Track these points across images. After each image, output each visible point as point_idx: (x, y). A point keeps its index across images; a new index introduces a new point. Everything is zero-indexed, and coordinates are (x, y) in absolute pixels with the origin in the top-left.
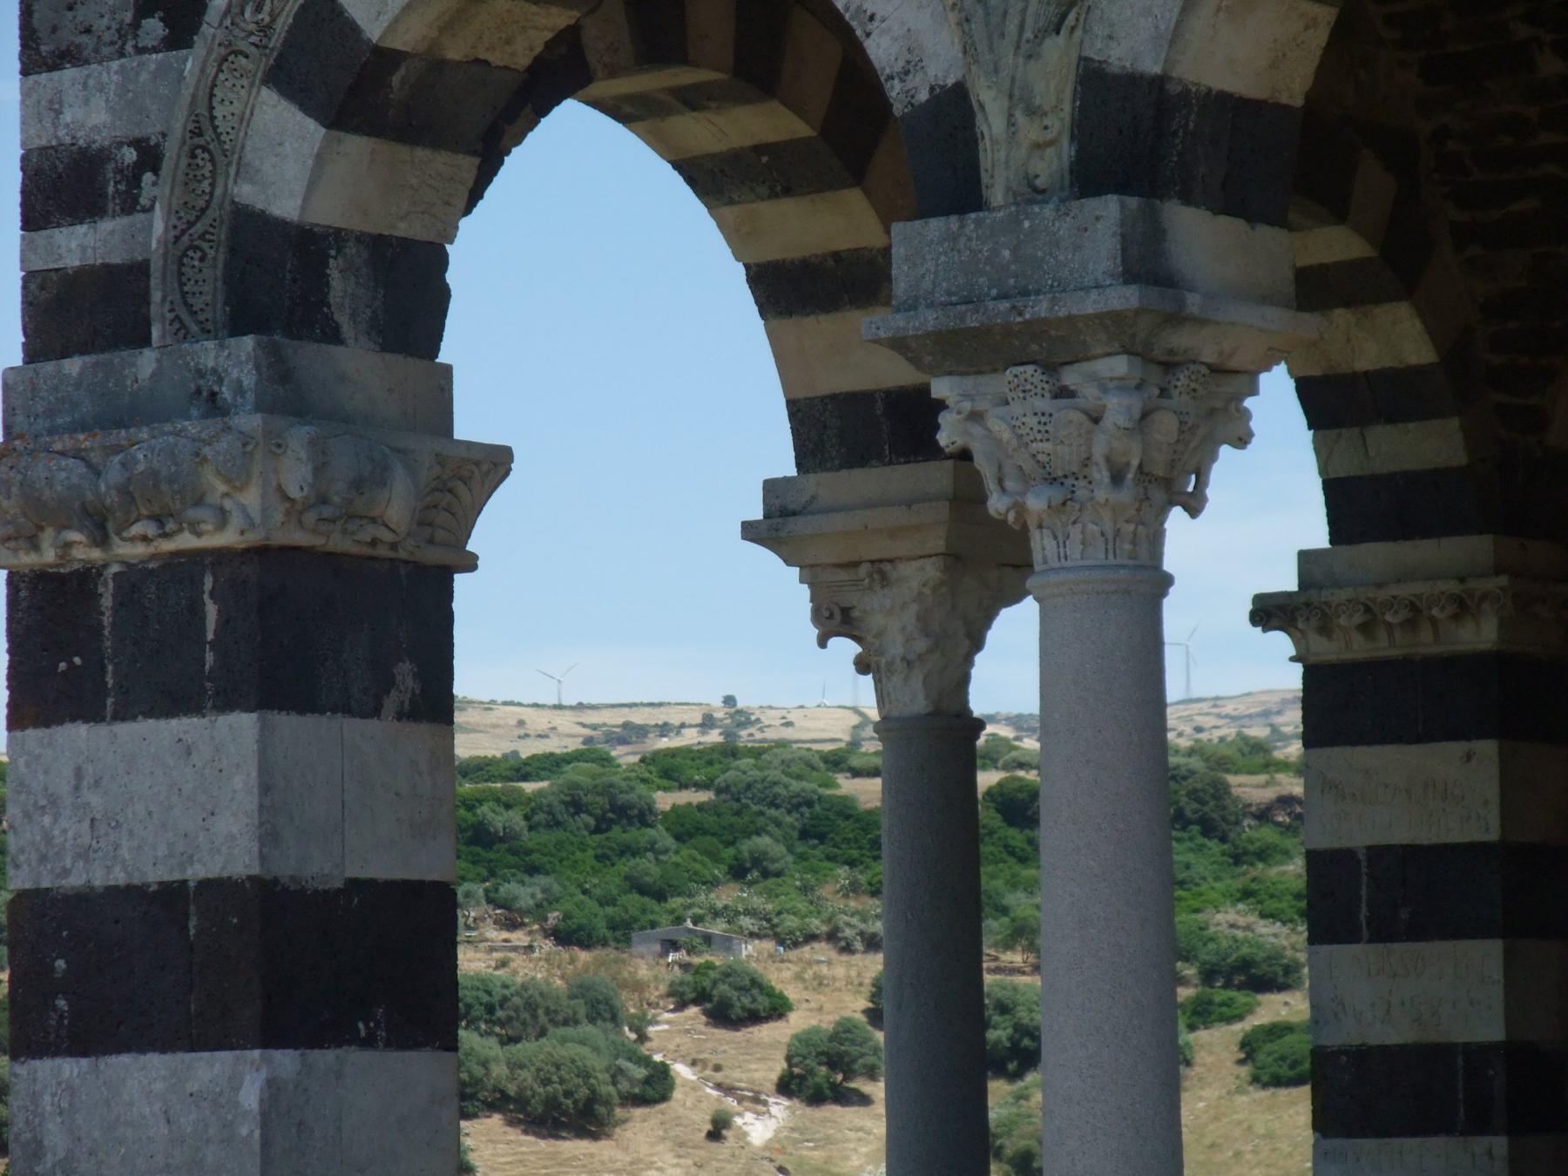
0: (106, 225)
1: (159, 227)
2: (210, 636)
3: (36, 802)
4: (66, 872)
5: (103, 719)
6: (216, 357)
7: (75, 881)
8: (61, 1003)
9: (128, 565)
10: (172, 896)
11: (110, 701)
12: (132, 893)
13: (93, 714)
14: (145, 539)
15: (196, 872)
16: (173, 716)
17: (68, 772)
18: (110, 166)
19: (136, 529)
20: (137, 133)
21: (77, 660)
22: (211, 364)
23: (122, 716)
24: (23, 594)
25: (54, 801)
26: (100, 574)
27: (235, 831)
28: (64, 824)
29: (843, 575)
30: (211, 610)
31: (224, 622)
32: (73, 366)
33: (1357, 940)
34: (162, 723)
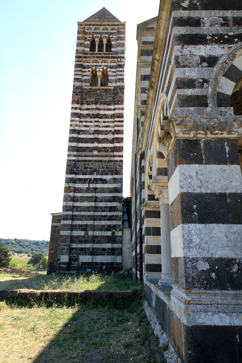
0: (196, 90)
1: (210, 90)
2: (227, 152)
3: (187, 177)
4: (195, 190)
5: (203, 164)
6: (225, 110)
7: (198, 191)
8: (196, 213)
9: (207, 139)
10: (223, 196)
11: (204, 161)
12: (214, 194)
13: (200, 162)
14: (217, 134)
15: (228, 192)
16: (220, 165)
17: (195, 172)
18: (197, 82)
19: (216, 132)
20: (202, 78)
21: (195, 154)
22: (224, 110)
23: (208, 163)
24: (181, 142)
25: (191, 177)
26: (200, 140)
27: (237, 185)
28: (194, 181)
29: (163, 187)
30: (227, 149)
31: (230, 151)
32: (192, 108)
33: (151, 235)
34: (217, 165)
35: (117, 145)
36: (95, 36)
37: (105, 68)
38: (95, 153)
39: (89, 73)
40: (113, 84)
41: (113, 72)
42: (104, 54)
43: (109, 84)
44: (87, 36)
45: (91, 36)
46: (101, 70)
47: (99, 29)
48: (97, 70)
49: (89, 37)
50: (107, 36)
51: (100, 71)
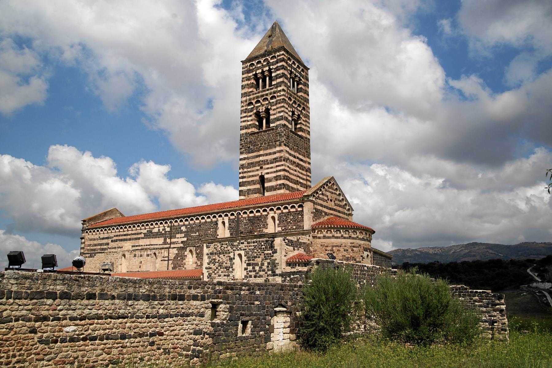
39: (290, 114)
44: (289, 68)
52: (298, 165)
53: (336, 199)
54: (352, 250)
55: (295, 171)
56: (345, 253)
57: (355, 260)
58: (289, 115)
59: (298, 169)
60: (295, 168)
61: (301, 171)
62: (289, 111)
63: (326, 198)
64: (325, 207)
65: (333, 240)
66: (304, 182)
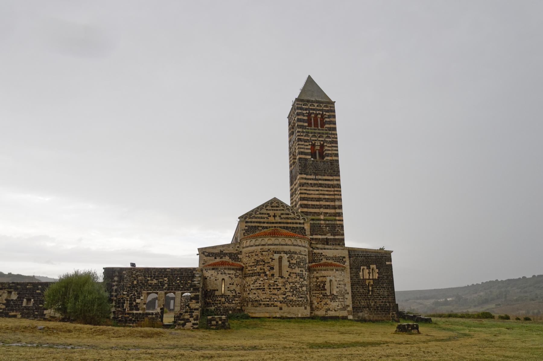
35: (338, 211)
36: (311, 112)
37: (322, 143)
38: (322, 217)
39: (309, 147)
40: (329, 158)
41: (328, 147)
42: (319, 130)
43: (326, 158)
44: (305, 112)
45: (308, 112)
46: (319, 144)
47: (314, 106)
48: (316, 144)
49: (306, 113)
50: (321, 112)
51: (318, 145)
52: (321, 185)
53: (282, 214)
54: (262, 254)
55: (317, 190)
56: (256, 257)
57: (264, 262)
58: (307, 149)
59: (321, 188)
60: (317, 188)
61: (326, 189)
62: (307, 145)
63: (267, 216)
64: (264, 223)
65: (249, 248)
66: (333, 197)
